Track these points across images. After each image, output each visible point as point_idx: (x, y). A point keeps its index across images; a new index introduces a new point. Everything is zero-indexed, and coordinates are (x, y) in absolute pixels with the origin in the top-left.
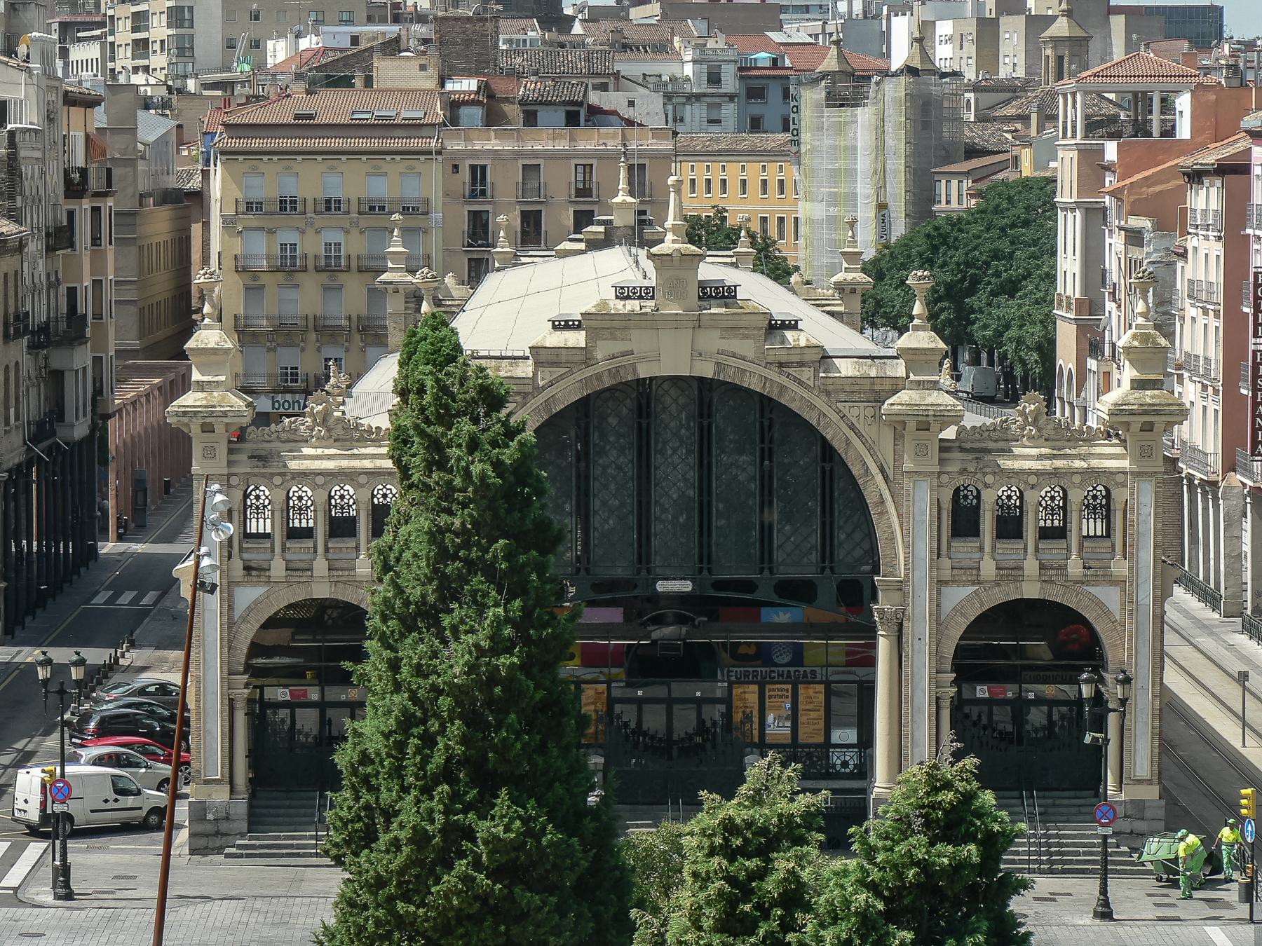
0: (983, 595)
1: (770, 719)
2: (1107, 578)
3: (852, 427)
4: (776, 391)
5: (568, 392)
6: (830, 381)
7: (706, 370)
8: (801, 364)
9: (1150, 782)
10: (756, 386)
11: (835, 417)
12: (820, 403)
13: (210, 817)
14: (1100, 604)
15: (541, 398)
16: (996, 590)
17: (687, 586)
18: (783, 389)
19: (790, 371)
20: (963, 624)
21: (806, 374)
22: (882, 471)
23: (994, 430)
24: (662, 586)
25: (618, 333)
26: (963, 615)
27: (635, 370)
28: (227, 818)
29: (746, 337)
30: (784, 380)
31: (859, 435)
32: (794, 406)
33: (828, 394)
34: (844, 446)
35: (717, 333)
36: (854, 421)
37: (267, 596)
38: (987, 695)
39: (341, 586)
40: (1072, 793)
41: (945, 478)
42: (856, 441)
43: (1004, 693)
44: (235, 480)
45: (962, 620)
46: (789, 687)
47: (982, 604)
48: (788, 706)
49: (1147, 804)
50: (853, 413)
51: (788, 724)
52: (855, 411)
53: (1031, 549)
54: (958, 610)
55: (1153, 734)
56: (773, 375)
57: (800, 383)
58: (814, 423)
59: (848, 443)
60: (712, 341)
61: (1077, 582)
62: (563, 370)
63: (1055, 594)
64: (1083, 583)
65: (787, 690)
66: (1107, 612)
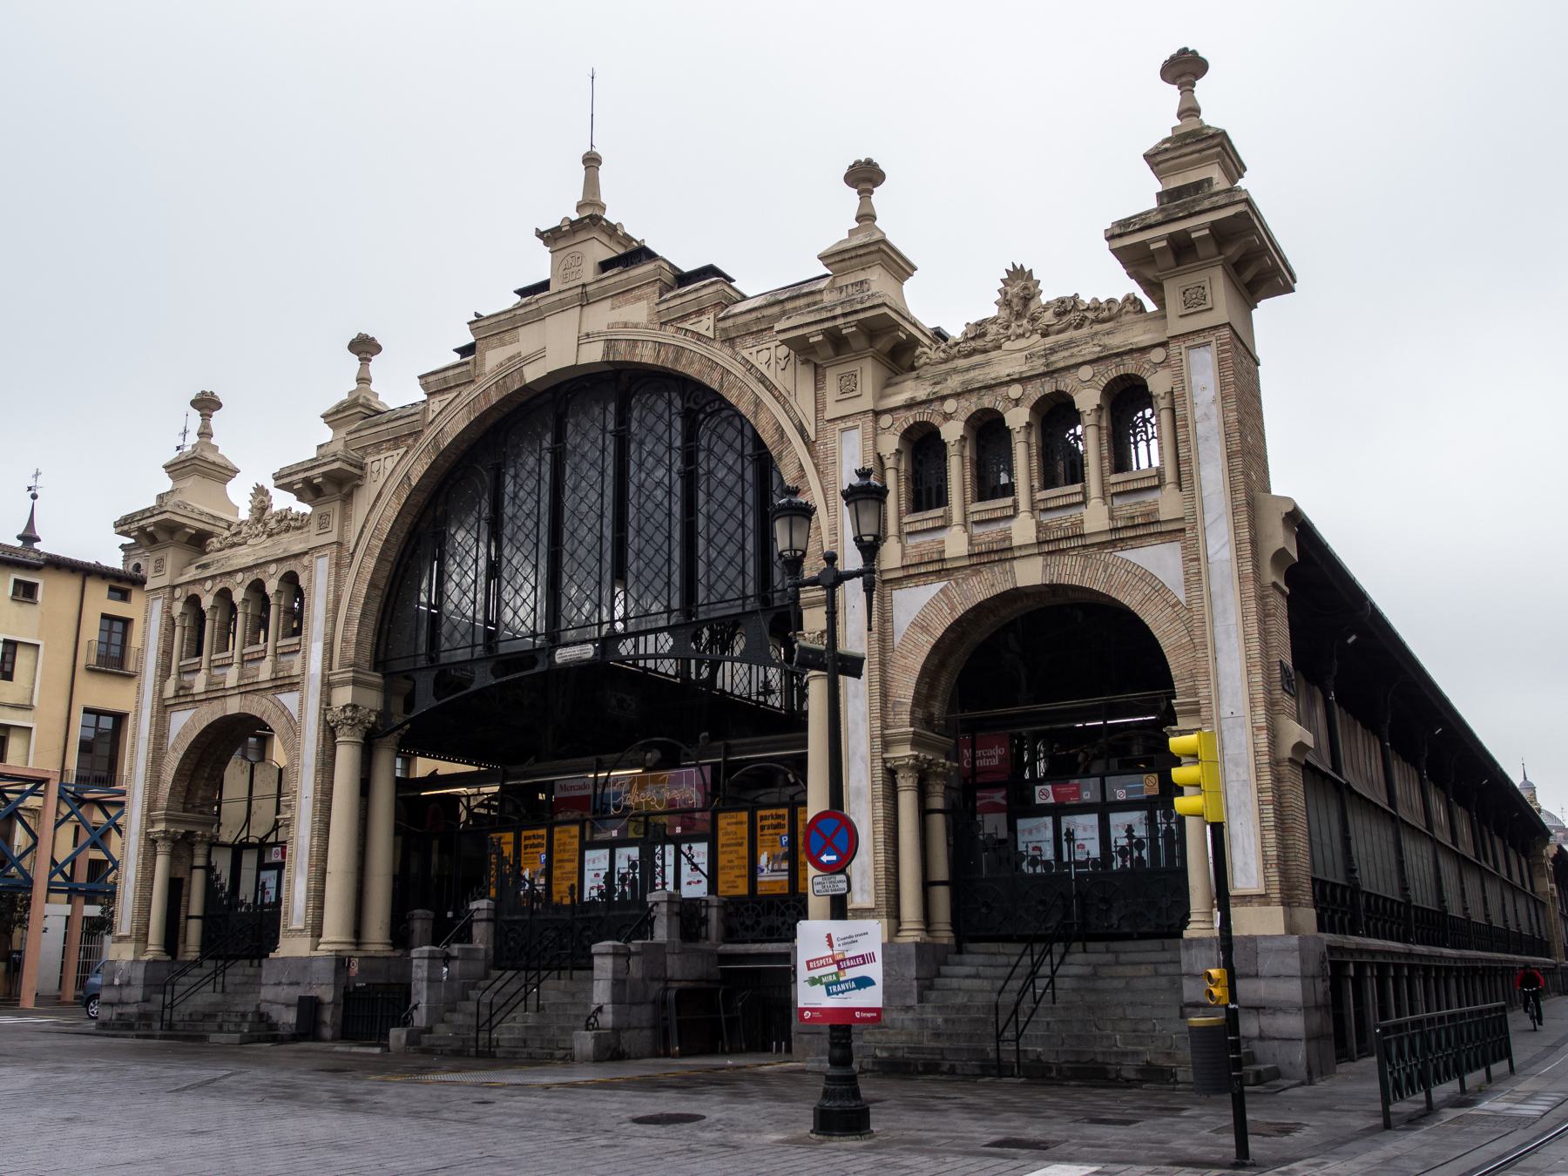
0: (953, 593)
1: (763, 859)
2: (1152, 529)
3: (763, 380)
4: (671, 356)
5: (453, 420)
6: (729, 323)
7: (593, 354)
8: (700, 312)
9: (1263, 899)
10: (646, 355)
11: (738, 370)
12: (721, 355)
13: (117, 982)
14: (1146, 577)
15: (429, 434)
16: (974, 581)
17: (588, 651)
18: (680, 350)
19: (686, 325)
20: (926, 643)
21: (705, 325)
22: (802, 431)
23: (967, 340)
24: (563, 655)
25: (507, 337)
26: (925, 629)
27: (522, 376)
28: (128, 984)
29: (639, 299)
30: (680, 340)
31: (770, 388)
32: (692, 371)
33: (730, 341)
34: (752, 408)
35: (608, 303)
36: (763, 368)
37: (192, 719)
38: (1051, 800)
39: (250, 697)
40: (1156, 943)
41: (886, 420)
42: (767, 398)
43: (1077, 793)
44: (178, 592)
45: (925, 637)
46: (784, 811)
47: (953, 609)
48: (785, 839)
49: (1262, 945)
50: (759, 361)
51: (785, 865)
52: (765, 355)
53: (1024, 504)
54: (920, 625)
55: (1261, 802)
56: (668, 335)
57: (699, 336)
58: (715, 386)
59: (758, 403)
60: (601, 317)
61: (1102, 545)
62: (451, 396)
63: (1072, 572)
64: (1112, 544)
65: (782, 817)
66: (1160, 589)
